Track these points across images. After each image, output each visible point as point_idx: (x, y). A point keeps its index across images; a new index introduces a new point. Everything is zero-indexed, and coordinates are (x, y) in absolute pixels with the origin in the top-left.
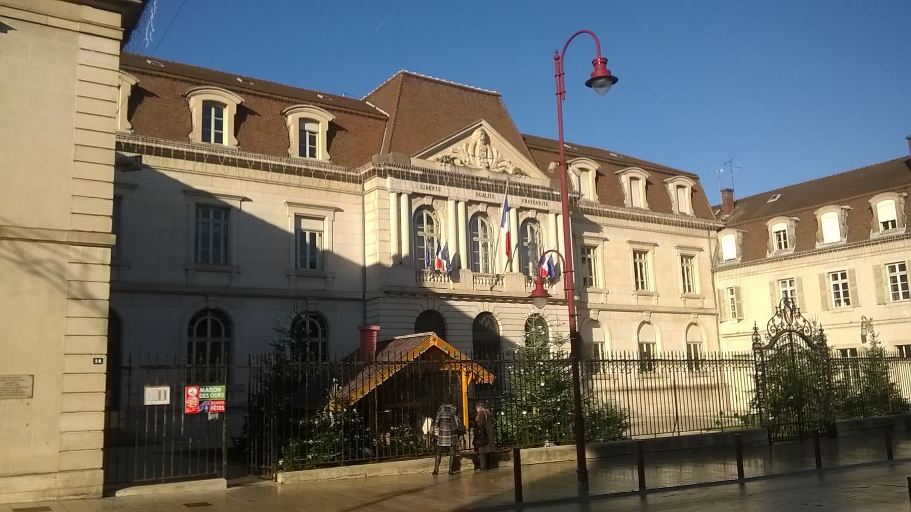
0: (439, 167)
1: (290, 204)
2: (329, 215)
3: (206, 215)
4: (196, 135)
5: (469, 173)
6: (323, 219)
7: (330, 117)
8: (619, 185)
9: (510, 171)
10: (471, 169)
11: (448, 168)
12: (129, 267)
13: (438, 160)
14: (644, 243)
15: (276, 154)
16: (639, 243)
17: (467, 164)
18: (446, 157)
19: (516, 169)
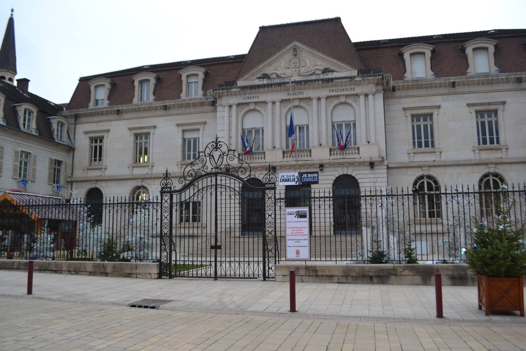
0: (257, 82)
1: (178, 125)
2: (201, 127)
3: (141, 139)
4: (136, 100)
5: (282, 81)
6: (199, 130)
7: (204, 70)
8: (466, 57)
9: (320, 72)
10: (284, 78)
11: (265, 82)
12: (105, 169)
13: (257, 78)
14: (489, 104)
15: (173, 98)
16: (482, 104)
17: (281, 75)
18: (264, 74)
19: (325, 69)
